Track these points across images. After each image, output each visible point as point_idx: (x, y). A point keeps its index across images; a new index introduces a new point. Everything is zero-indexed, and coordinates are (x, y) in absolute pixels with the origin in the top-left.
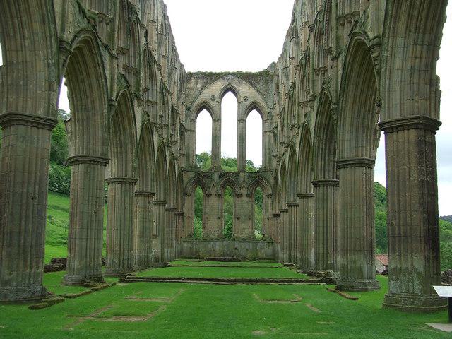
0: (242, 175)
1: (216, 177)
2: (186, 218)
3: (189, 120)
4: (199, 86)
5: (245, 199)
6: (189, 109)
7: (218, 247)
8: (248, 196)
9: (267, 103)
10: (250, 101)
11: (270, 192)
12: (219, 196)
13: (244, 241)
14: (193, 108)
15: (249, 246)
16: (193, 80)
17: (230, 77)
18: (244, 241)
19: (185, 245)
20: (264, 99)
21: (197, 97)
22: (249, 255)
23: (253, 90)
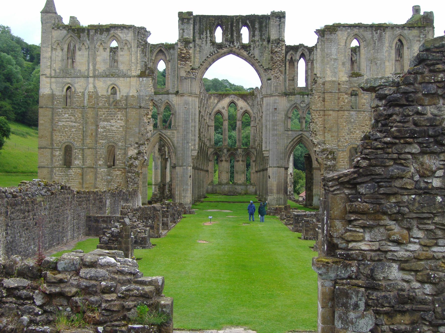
0: (239, 150)
1: (225, 151)
2: (209, 173)
3: (210, 120)
4: (216, 101)
5: (241, 163)
6: (210, 114)
7: (226, 188)
8: (242, 161)
9: (253, 110)
10: (244, 110)
11: (254, 159)
12: (226, 161)
13: (240, 185)
14: (213, 114)
15: (243, 187)
16: (212, 97)
17: (233, 96)
18: (240, 185)
19: (209, 187)
20: (251, 108)
21: (214, 108)
22: (243, 192)
23: (245, 104)
